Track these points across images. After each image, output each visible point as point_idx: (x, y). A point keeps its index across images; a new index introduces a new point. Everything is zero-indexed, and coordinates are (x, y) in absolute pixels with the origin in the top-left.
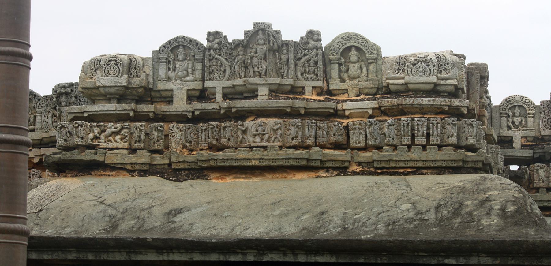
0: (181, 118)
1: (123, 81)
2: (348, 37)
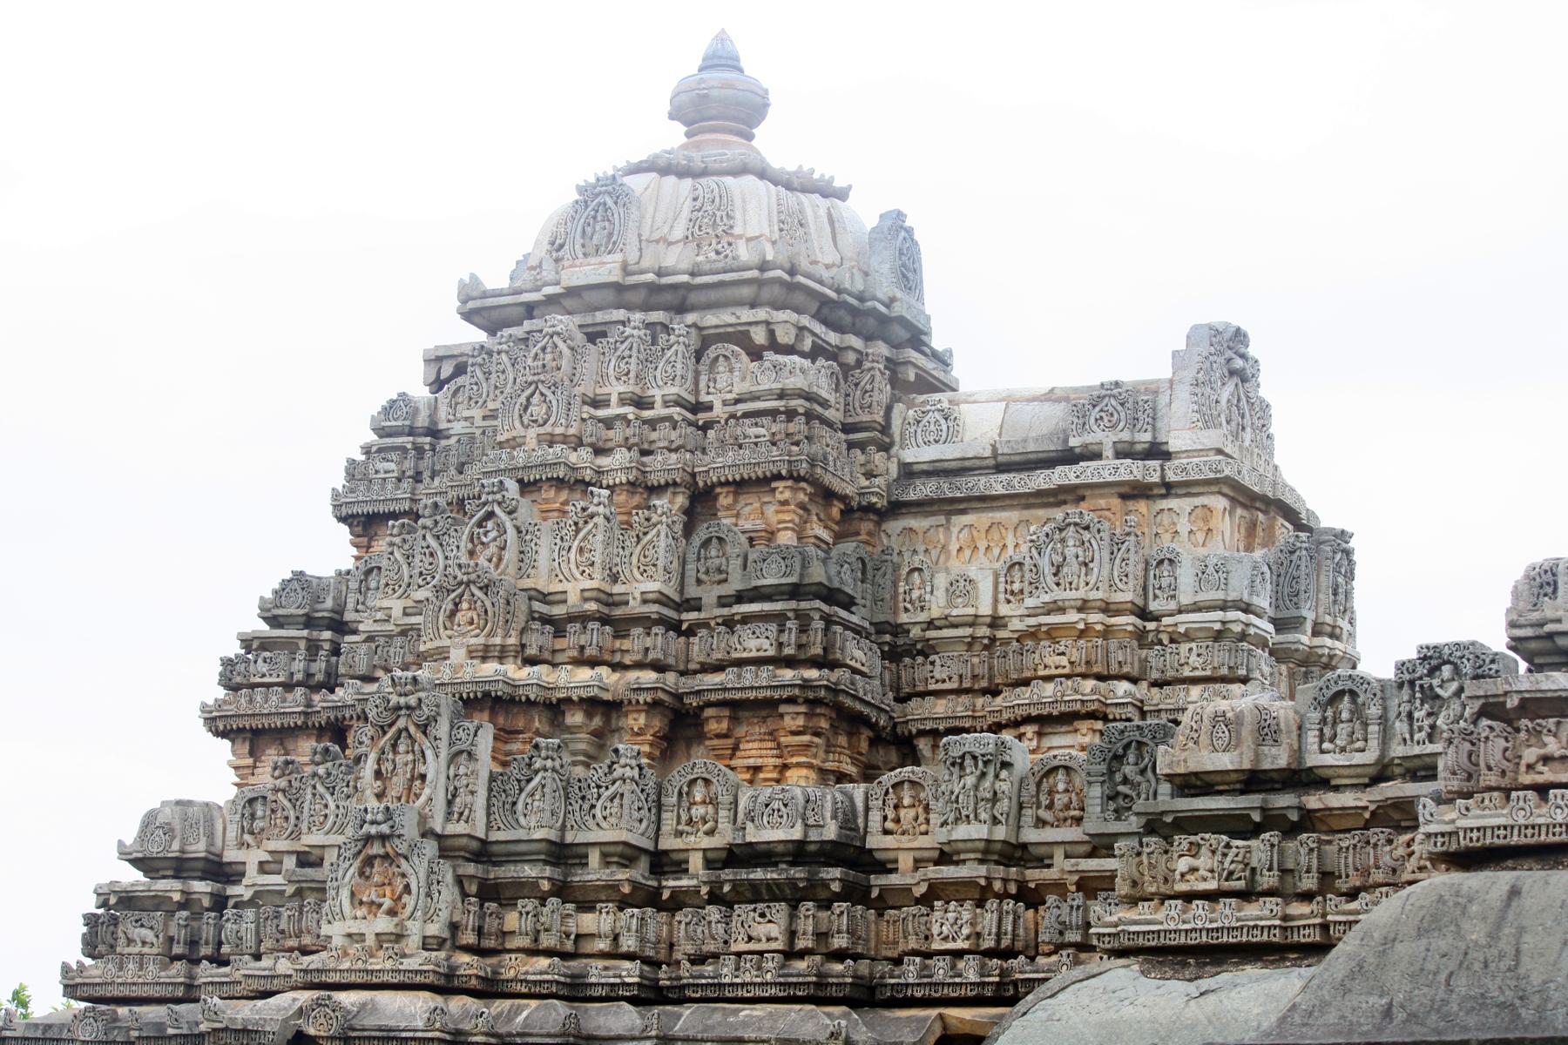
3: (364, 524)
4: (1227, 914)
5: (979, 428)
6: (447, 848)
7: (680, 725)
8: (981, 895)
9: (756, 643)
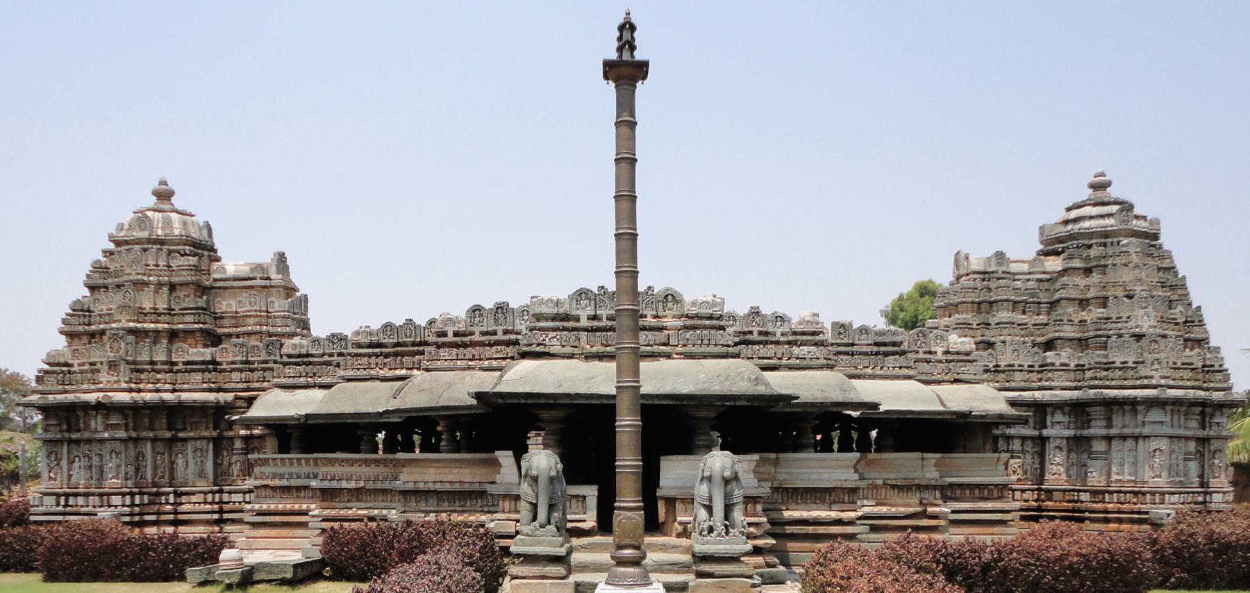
0: (585, 329)
1: (555, 311)
6: (128, 363)
7: (173, 335)
8: (241, 371)
9: (190, 319)
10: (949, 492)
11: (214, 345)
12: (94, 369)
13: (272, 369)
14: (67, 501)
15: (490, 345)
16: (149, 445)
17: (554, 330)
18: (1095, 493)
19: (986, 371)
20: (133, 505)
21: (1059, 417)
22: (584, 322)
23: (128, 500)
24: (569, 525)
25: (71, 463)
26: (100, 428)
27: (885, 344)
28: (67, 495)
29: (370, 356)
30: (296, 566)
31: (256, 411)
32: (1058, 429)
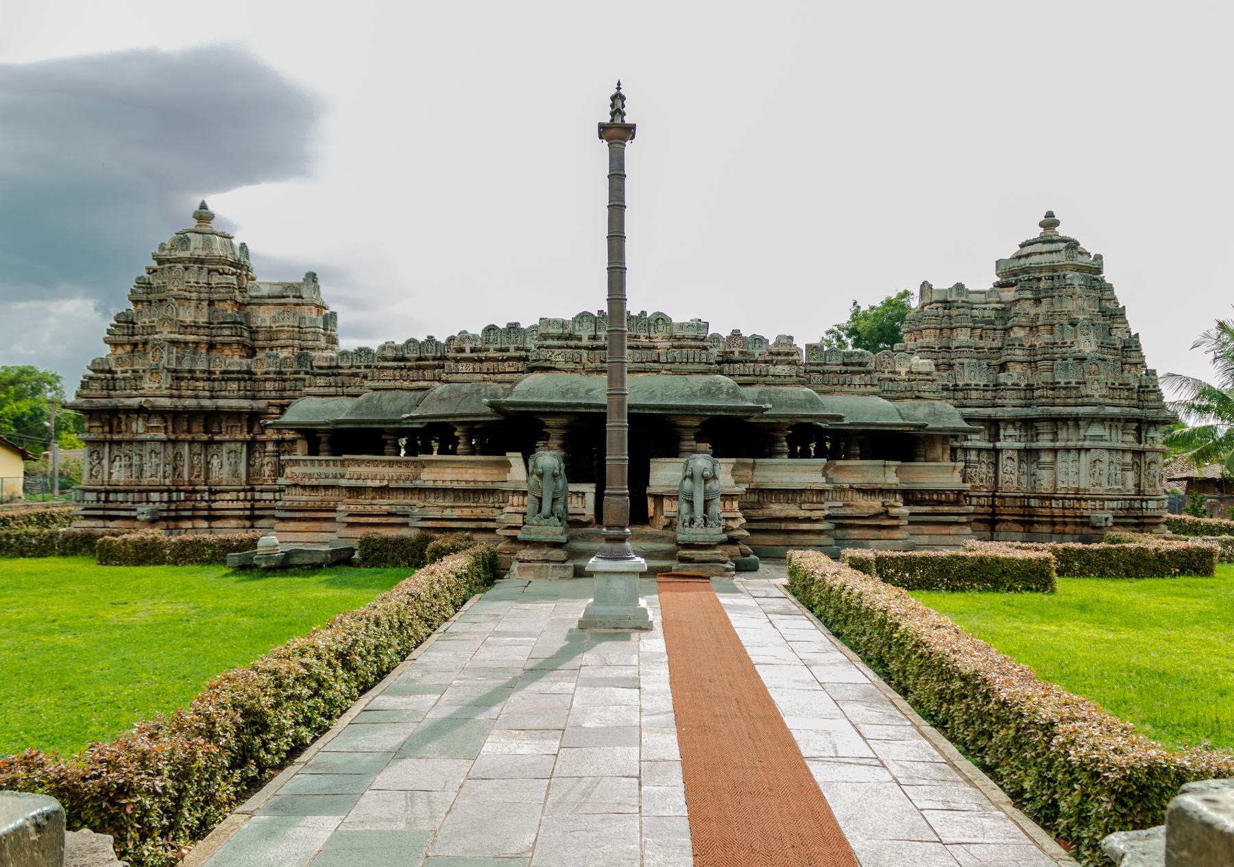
0: (587, 348)
1: (561, 331)
2: (658, 313)
3: (136, 302)
4: (326, 390)
5: (265, 291)
6: (169, 370)
7: (211, 346)
8: (275, 380)
9: (227, 332)
10: (909, 496)
11: (248, 357)
12: (137, 376)
13: (304, 380)
14: (107, 498)
15: (503, 360)
16: (187, 447)
17: (559, 347)
18: (1043, 498)
19: (945, 388)
20: (170, 501)
21: (1011, 431)
22: (585, 342)
23: (165, 496)
24: (571, 518)
25: (112, 462)
26: (141, 430)
27: (852, 364)
28: (107, 492)
29: (395, 369)
30: (326, 552)
31: (289, 417)
32: (1010, 441)
